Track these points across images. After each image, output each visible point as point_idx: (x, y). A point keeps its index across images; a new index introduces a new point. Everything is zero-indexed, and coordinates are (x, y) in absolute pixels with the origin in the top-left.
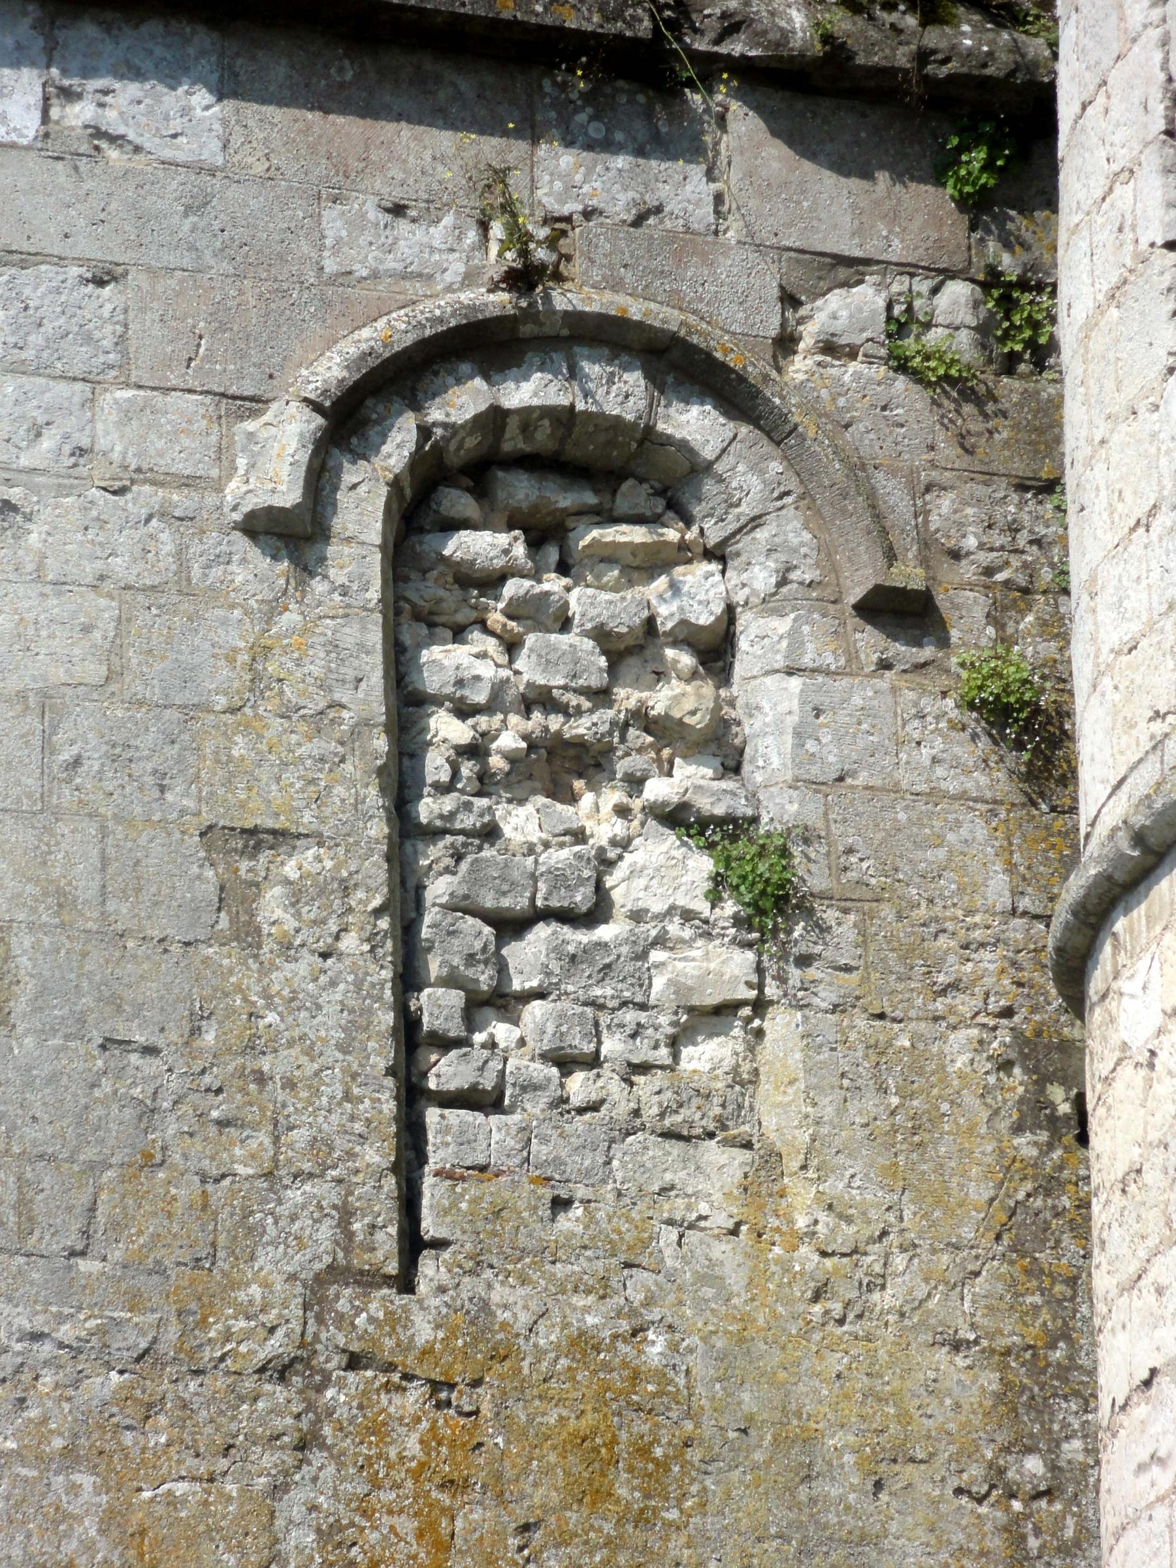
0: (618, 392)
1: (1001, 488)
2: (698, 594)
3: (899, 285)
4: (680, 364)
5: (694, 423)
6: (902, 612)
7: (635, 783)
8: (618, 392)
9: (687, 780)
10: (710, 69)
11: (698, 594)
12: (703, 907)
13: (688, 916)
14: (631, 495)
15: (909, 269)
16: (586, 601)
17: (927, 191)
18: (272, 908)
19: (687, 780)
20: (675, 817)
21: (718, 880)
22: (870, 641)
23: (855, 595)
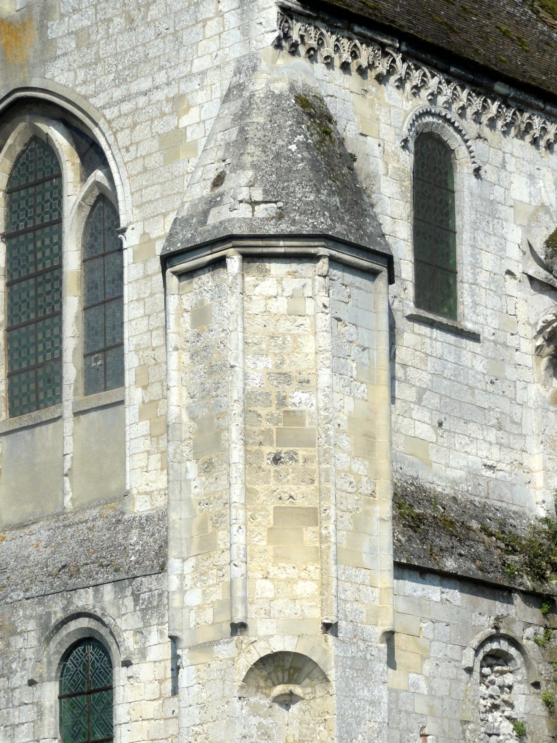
0: (504, 645)
1: (547, 664)
2: (509, 679)
3: (537, 628)
4: (513, 642)
5: (513, 651)
6: (536, 685)
7: (503, 712)
8: (504, 645)
9: (508, 712)
10: (517, 591)
11: (509, 679)
12: (511, 733)
13: (510, 734)
14: (501, 661)
15: (537, 625)
16: (499, 680)
17: (539, 610)
18: (468, 734)
19: (508, 712)
20: (508, 718)
21: (514, 729)
22: (533, 689)
23: (532, 682)
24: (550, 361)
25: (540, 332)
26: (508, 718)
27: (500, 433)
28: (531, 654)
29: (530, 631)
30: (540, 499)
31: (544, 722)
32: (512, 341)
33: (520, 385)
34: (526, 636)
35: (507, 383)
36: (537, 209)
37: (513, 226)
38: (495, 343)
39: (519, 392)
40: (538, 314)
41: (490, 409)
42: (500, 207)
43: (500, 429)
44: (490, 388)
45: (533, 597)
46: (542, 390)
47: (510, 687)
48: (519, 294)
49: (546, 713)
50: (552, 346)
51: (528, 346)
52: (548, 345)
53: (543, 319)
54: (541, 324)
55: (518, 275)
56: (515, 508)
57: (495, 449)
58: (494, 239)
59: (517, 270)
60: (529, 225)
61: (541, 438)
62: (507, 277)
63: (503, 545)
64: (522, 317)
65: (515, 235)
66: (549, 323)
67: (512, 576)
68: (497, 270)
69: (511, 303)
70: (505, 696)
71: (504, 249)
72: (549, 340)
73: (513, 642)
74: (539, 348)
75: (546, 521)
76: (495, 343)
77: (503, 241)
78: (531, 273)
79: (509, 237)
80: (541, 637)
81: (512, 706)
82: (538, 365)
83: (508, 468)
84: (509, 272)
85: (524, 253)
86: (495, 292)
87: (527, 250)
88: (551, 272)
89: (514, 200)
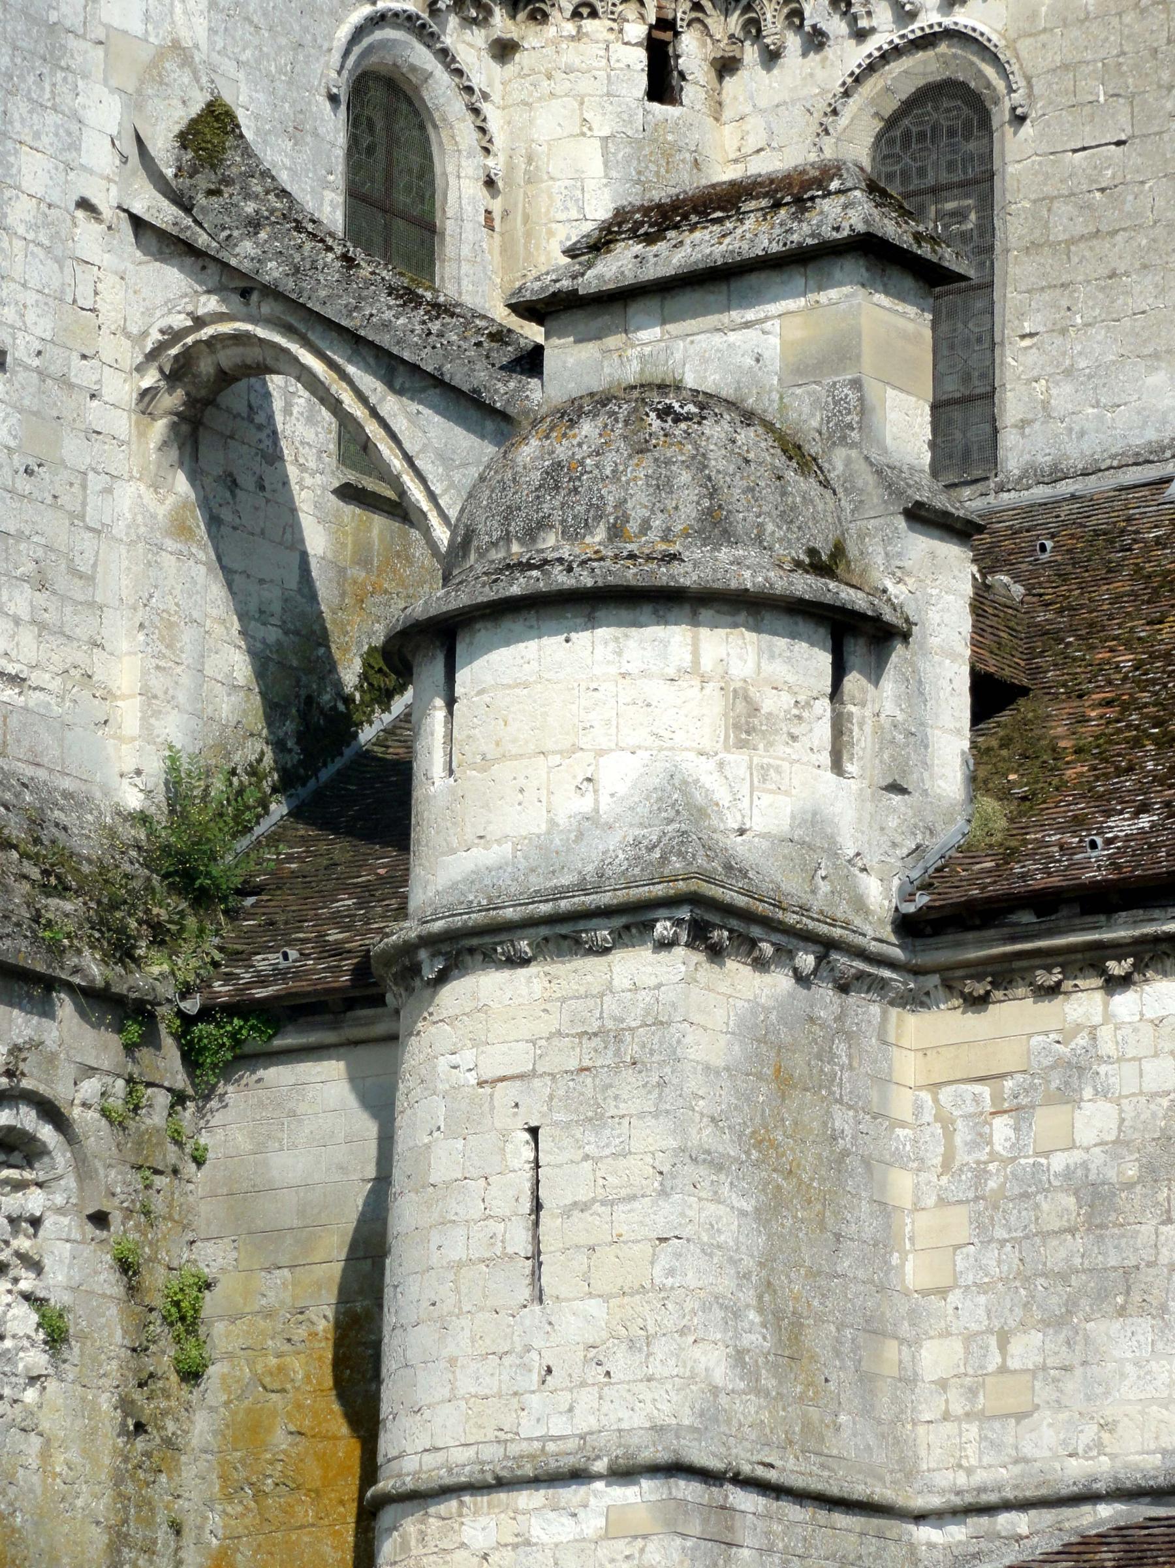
0: (26, 1118)
1: (127, 1168)
2: (34, 1201)
3: (110, 1080)
4: (50, 1112)
5: (46, 1133)
6: (100, 1219)
7: (16, 1281)
8: (26, 1118)
11: (34, 1201)
12: (33, 1334)
13: (29, 1337)
14: (16, 1157)
15: (108, 1073)
17: (116, 1037)
20: (27, 1297)
21: (39, 1325)
22: (89, 1228)
23: (90, 1211)
24: (174, 427)
25: (152, 356)
26: (27, 1297)
27: (41, 598)
28: (91, 1143)
29: (90, 1088)
30: (129, 766)
31: (113, 1311)
32: (83, 374)
33: (95, 482)
34: (82, 1097)
35: (65, 475)
36: (161, 55)
37: (100, 90)
38: (42, 374)
39: (92, 500)
40: (148, 312)
41: (20, 536)
42: (72, 43)
43: (42, 587)
44: (24, 484)
45: (103, 1004)
46: (148, 496)
47: (36, 1222)
48: (107, 260)
49: (118, 1291)
50: (180, 393)
51: (122, 389)
52: (171, 390)
53: (163, 323)
54: (155, 336)
55: (107, 212)
56: (67, 784)
57: (27, 636)
58: (52, 118)
59: (105, 202)
60: (139, 92)
61: (140, 615)
62: (80, 214)
63: (35, 873)
64: (109, 315)
65: (105, 114)
66: (176, 336)
67: (55, 950)
68: (55, 196)
69: (86, 277)
70: (23, 1243)
71: (75, 146)
72: (176, 375)
73: (50, 1112)
74: (146, 395)
75: (143, 818)
76: (42, 374)
77: (74, 127)
78: (138, 209)
79: (90, 116)
80: (116, 1103)
81: (36, 1267)
82: (142, 434)
83: (55, 685)
84: (84, 204)
85: (125, 160)
86: (48, 250)
87: (132, 151)
88: (188, 210)
89: (108, 27)
